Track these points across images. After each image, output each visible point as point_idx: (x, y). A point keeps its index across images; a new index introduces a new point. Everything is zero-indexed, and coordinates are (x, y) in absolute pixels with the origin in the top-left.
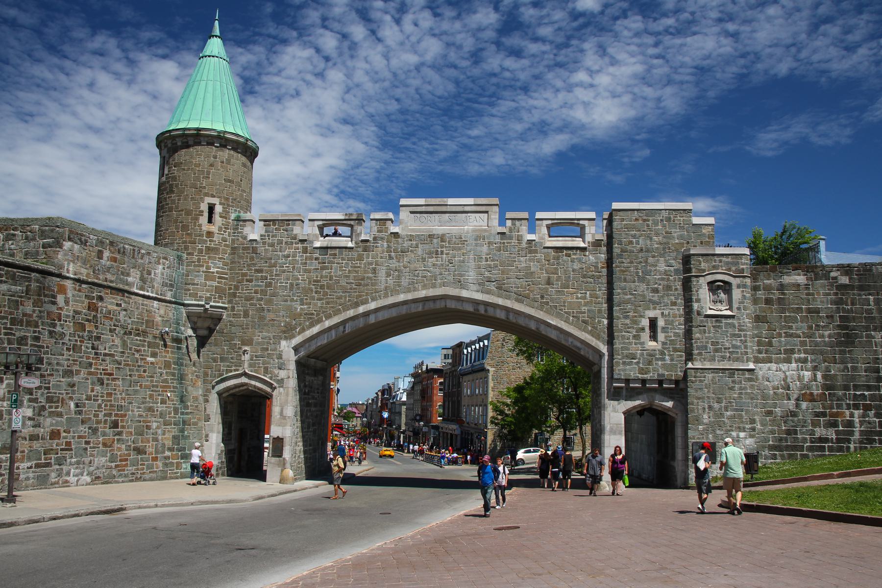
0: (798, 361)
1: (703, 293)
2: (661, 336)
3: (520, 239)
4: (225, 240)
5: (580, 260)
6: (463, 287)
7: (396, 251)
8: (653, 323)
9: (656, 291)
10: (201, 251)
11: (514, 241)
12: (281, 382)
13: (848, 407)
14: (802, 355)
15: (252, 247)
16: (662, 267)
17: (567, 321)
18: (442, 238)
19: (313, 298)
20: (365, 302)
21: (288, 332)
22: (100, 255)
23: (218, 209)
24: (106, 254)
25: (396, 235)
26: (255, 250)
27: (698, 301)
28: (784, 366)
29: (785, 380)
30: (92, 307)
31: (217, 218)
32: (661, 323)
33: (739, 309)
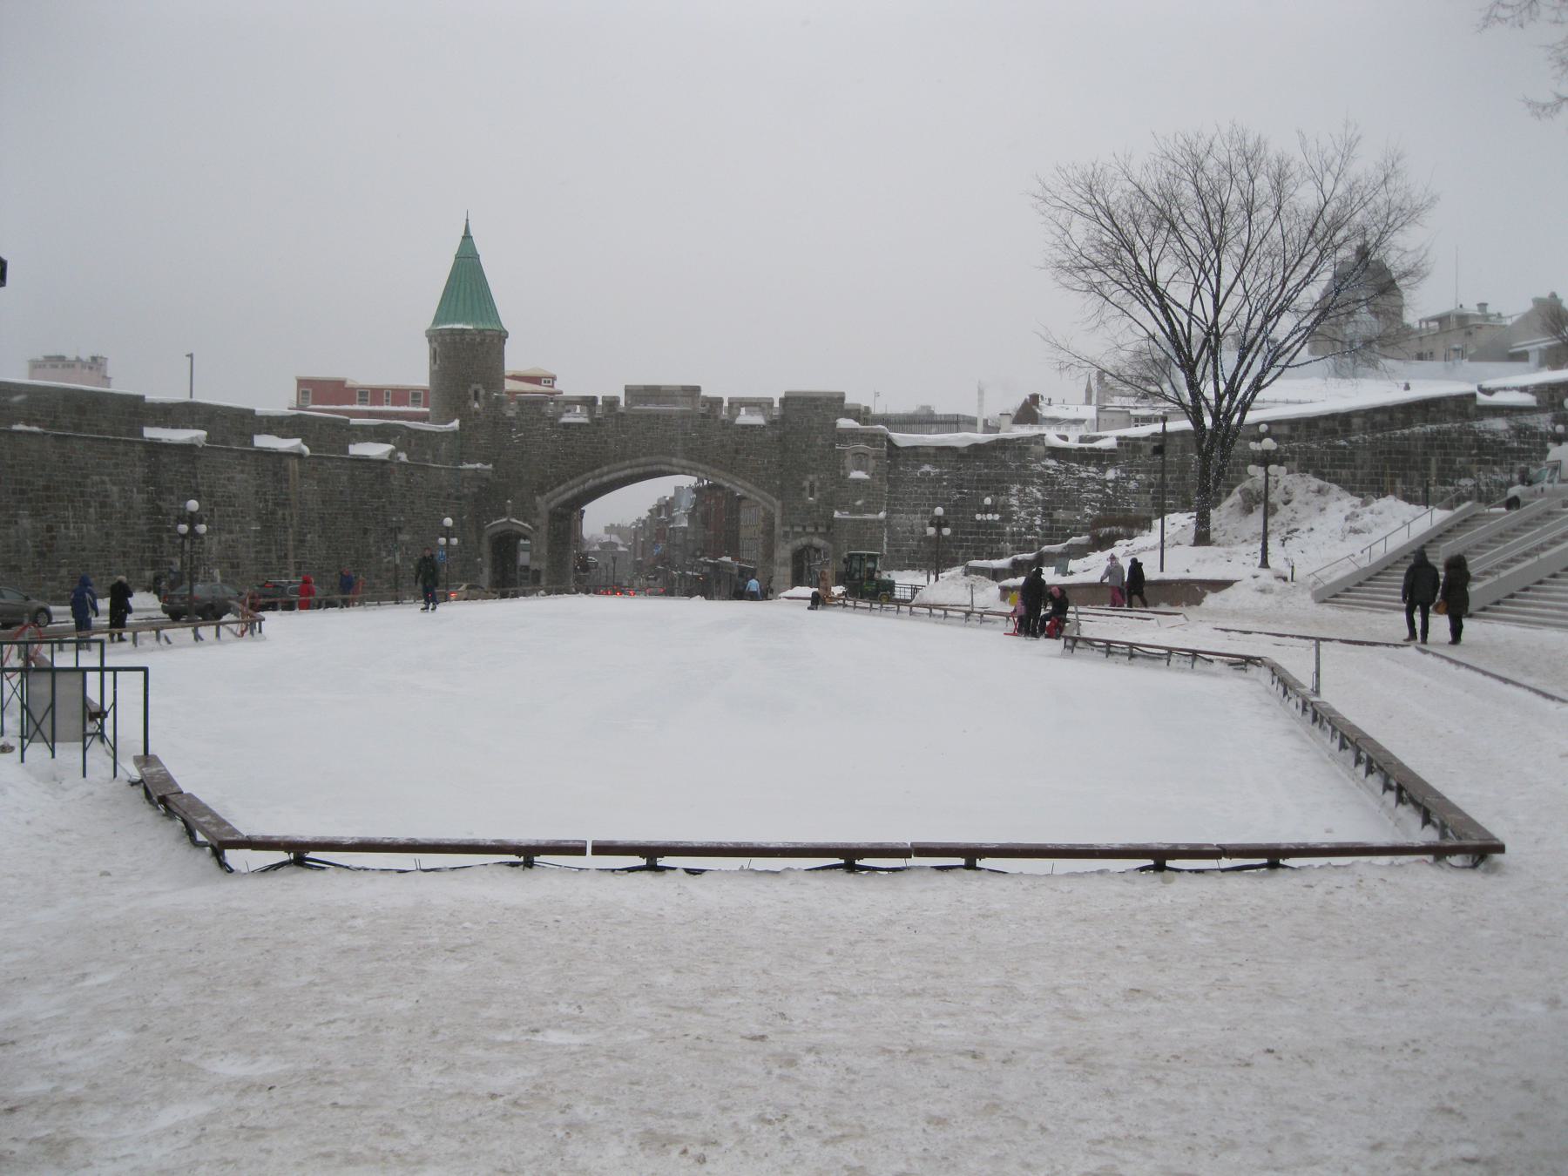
0: (923, 512)
1: (849, 461)
2: (817, 495)
3: (716, 417)
4: (488, 416)
5: (760, 435)
6: (673, 455)
7: (622, 426)
8: (812, 486)
9: (815, 460)
10: (471, 427)
11: (711, 420)
12: (536, 528)
13: (955, 547)
14: (927, 508)
15: (510, 423)
16: (820, 441)
17: (750, 482)
18: (658, 416)
19: (559, 463)
20: (599, 467)
21: (542, 490)
22: (410, 442)
23: (482, 392)
24: (413, 443)
25: (622, 414)
26: (512, 425)
27: (844, 468)
28: (912, 517)
29: (912, 526)
30: (408, 481)
31: (482, 400)
32: (817, 484)
33: (873, 474)
